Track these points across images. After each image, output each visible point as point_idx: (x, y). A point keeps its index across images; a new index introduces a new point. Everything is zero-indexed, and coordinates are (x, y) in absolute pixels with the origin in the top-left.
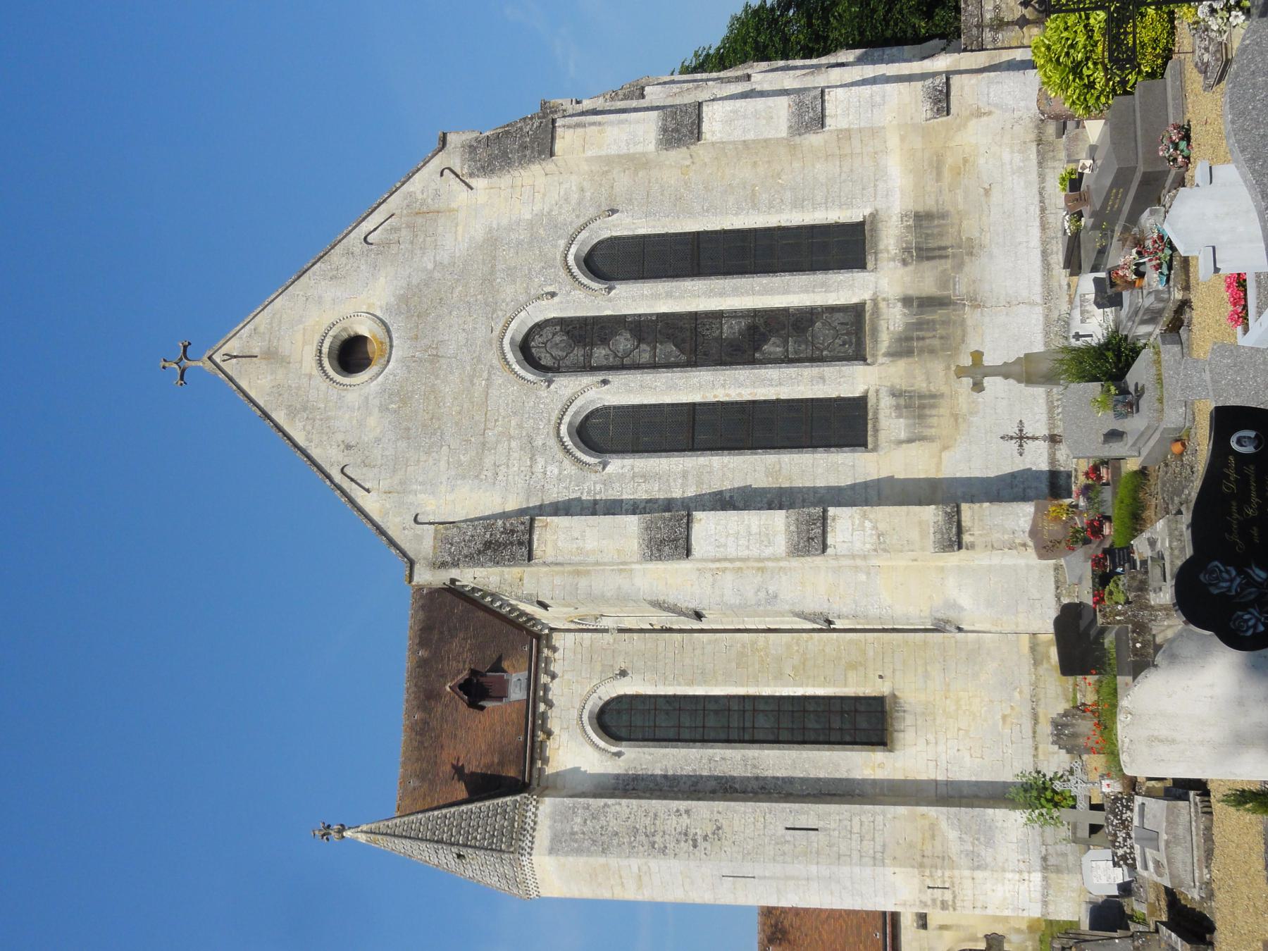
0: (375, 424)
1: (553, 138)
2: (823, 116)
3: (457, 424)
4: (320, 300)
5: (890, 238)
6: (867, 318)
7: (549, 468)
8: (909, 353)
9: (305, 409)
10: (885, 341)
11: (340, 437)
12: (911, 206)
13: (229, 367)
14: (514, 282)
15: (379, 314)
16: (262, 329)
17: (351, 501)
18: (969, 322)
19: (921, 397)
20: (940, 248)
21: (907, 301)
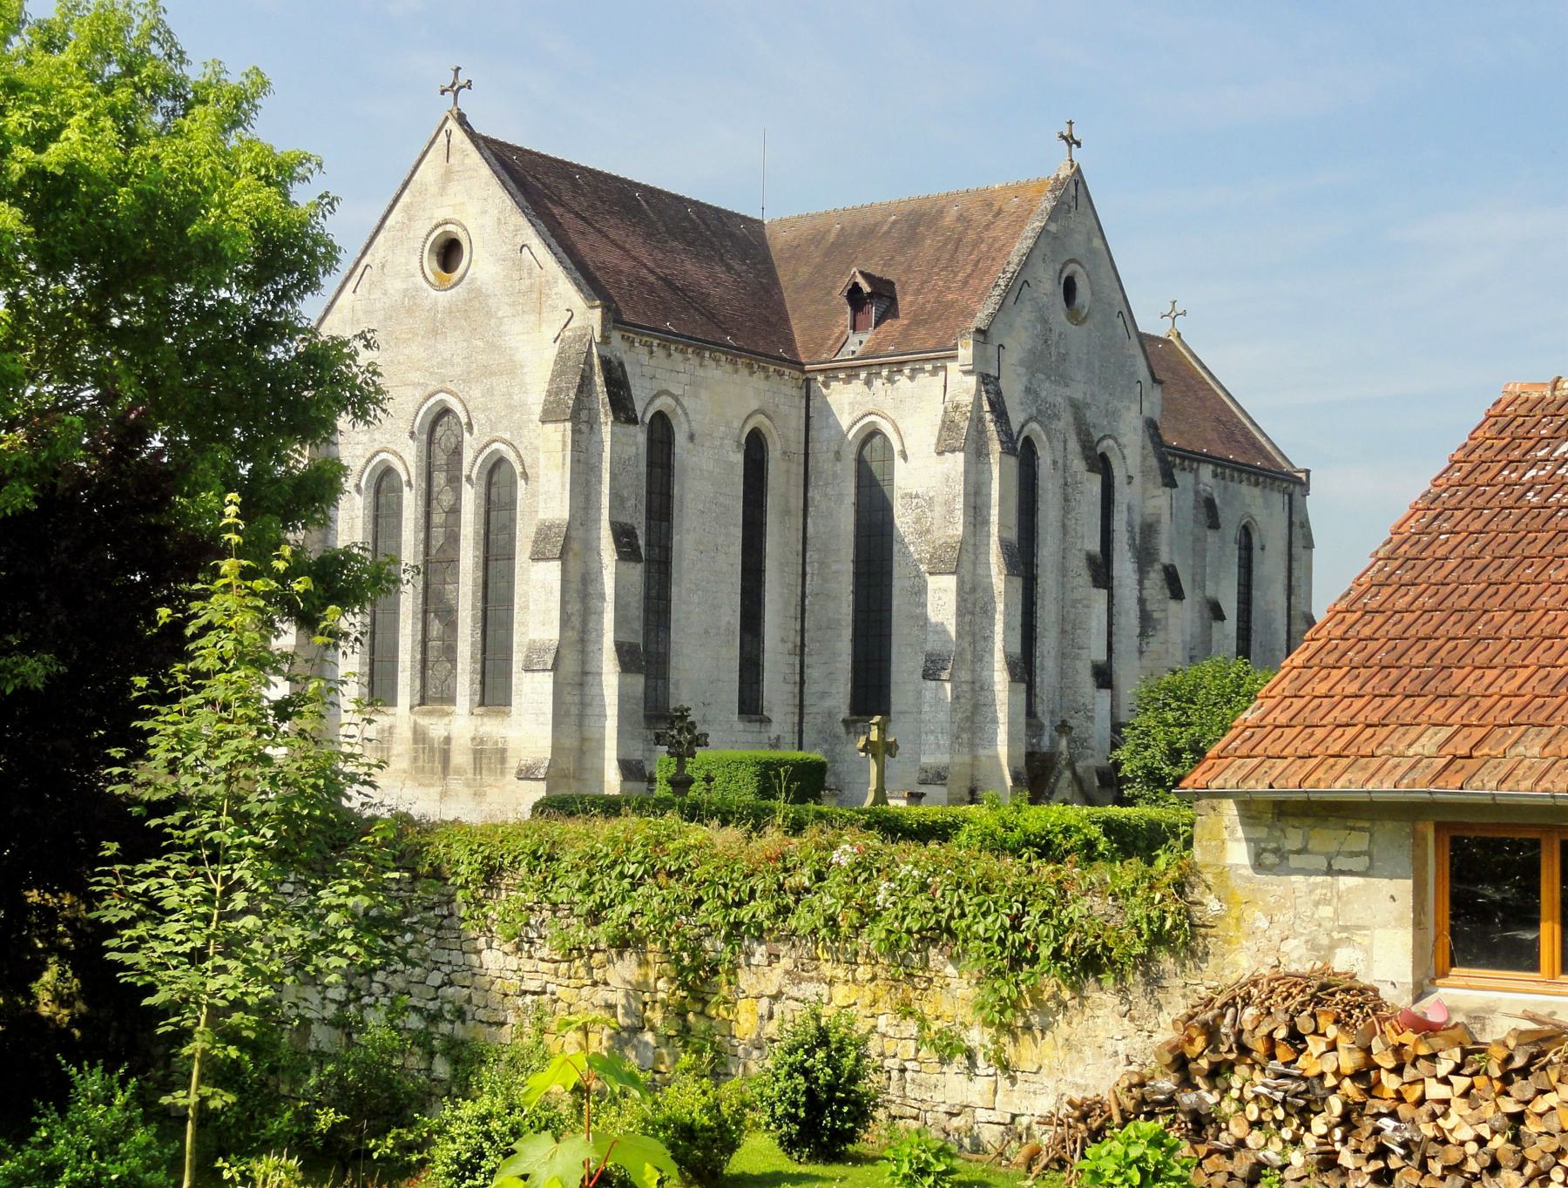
0: (395, 286)
1: (556, 421)
2: (533, 671)
3: (392, 361)
4: (484, 212)
5: (492, 727)
6: (446, 707)
7: (360, 446)
8: (415, 741)
9: (409, 220)
10: (424, 721)
11: (389, 258)
12: (511, 746)
13: (442, 137)
14: (483, 396)
15: (469, 274)
16: (467, 161)
17: (347, 279)
18: (432, 790)
19: (388, 749)
20: (481, 769)
21: (448, 740)
